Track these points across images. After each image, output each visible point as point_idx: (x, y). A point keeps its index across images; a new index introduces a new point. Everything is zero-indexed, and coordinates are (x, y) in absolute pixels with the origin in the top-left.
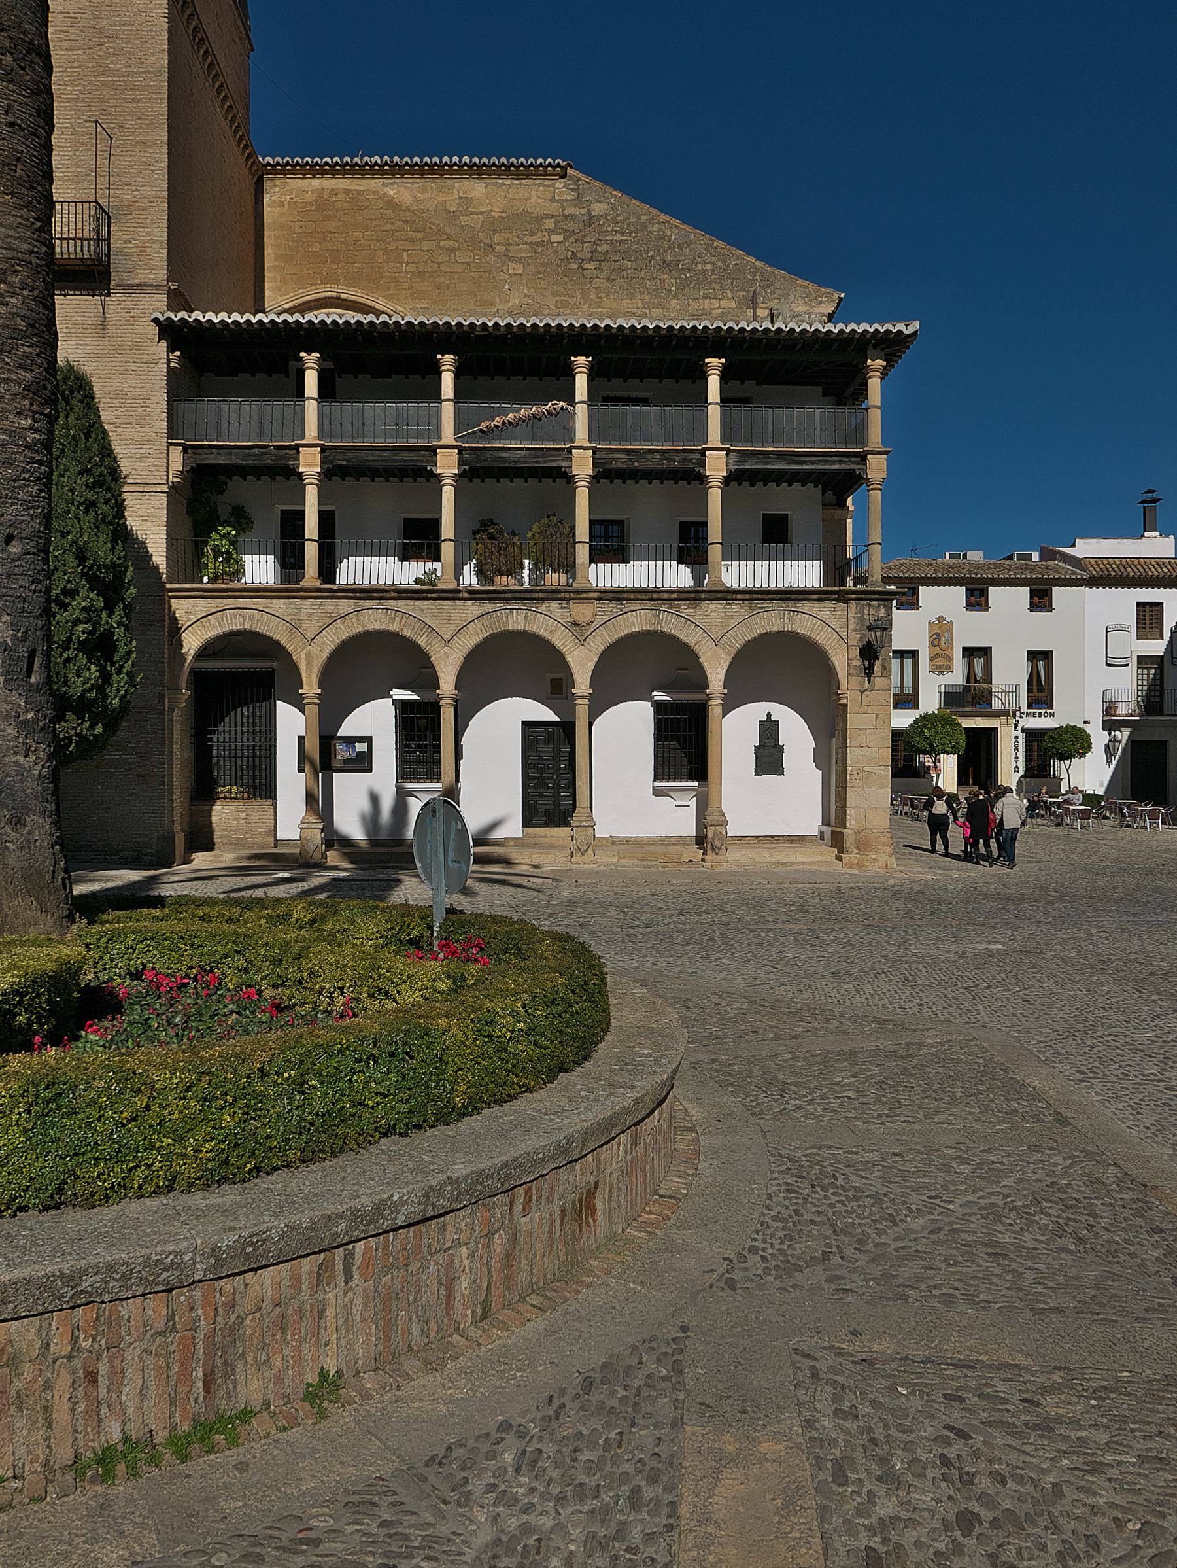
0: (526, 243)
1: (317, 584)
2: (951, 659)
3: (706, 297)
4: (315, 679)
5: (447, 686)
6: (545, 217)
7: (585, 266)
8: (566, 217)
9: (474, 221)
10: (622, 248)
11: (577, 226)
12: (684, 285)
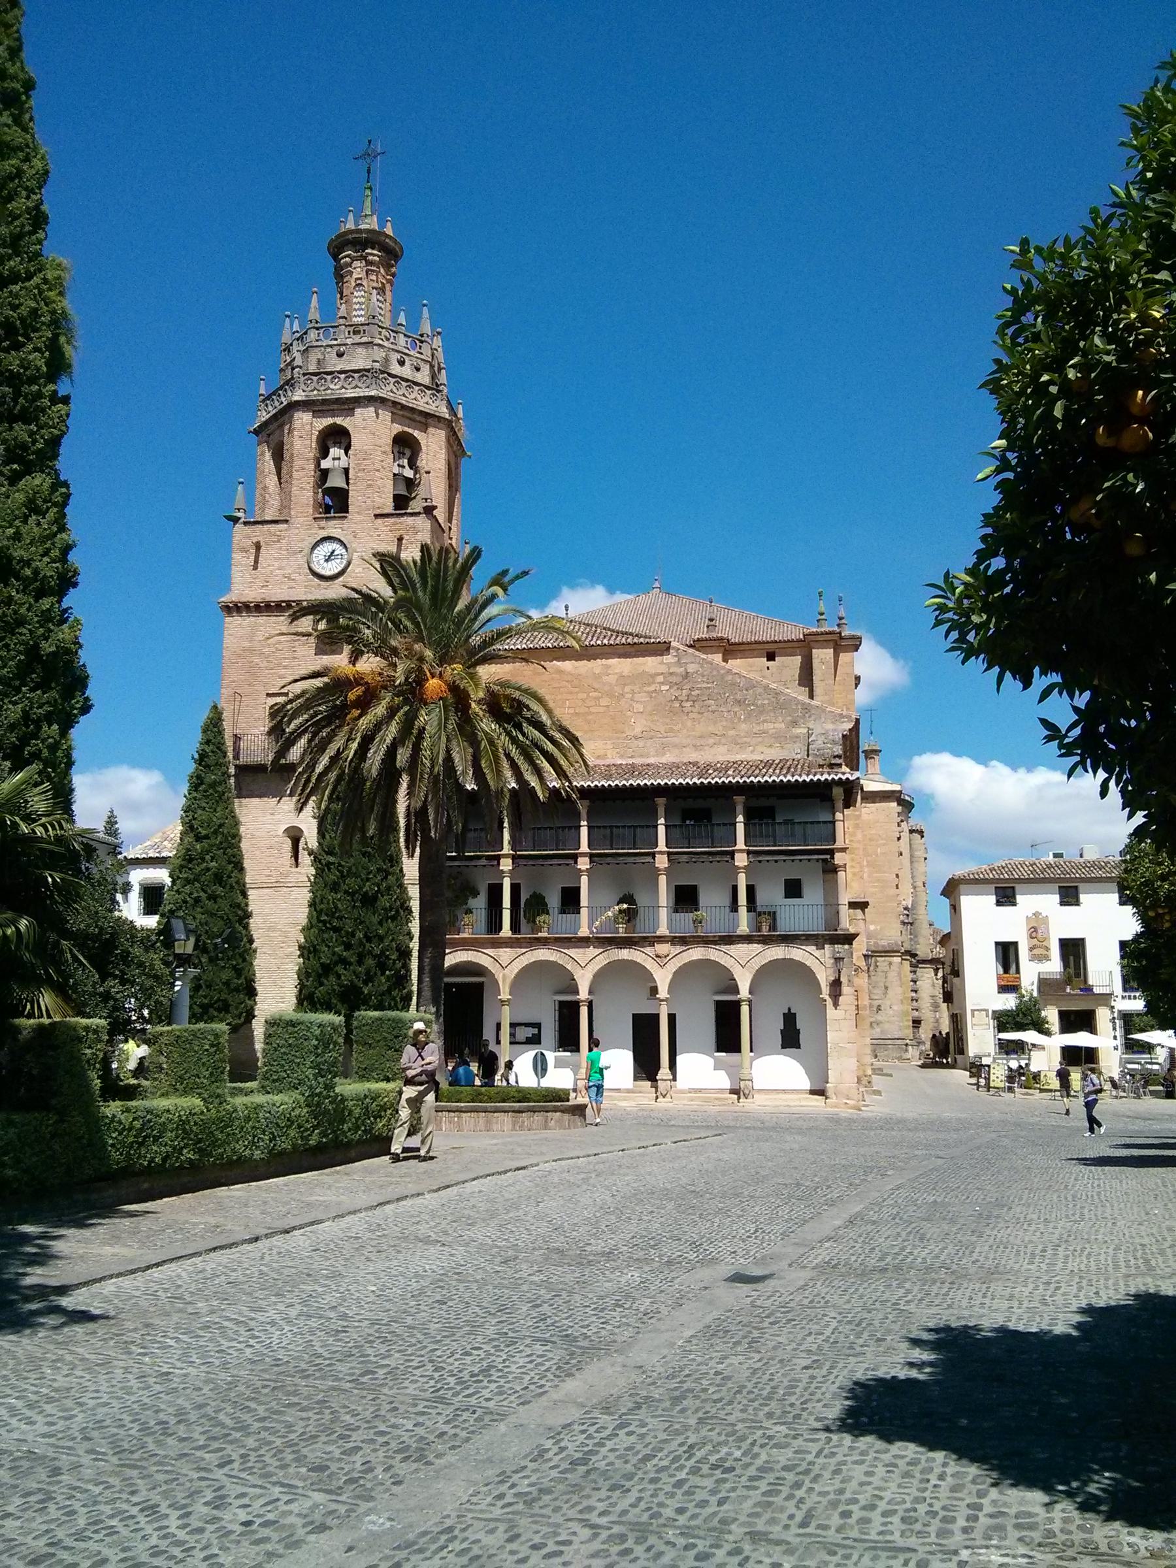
2: (1047, 949)
3: (765, 721)
4: (507, 990)
5: (583, 994)
6: (659, 674)
7: (684, 704)
8: (671, 674)
10: (708, 692)
11: (679, 679)
12: (749, 715)
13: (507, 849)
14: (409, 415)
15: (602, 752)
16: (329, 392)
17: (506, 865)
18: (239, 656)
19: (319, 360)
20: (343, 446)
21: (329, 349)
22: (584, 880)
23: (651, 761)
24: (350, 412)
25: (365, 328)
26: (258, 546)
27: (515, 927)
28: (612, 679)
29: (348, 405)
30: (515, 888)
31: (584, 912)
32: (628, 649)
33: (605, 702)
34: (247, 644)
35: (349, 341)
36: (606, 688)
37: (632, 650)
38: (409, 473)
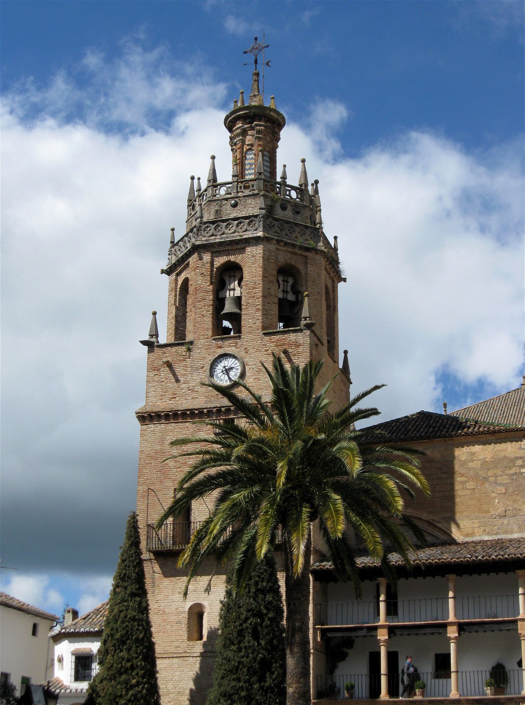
0: (506, 475)
1: (387, 698)
6: (517, 458)
9: (476, 464)
13: (382, 619)
14: (290, 250)
15: (470, 531)
16: (223, 236)
17: (382, 635)
18: (152, 458)
19: (217, 211)
20: (238, 277)
21: (224, 202)
22: (453, 646)
23: (516, 536)
24: (242, 250)
25: (252, 183)
26: (169, 365)
27: (393, 691)
28: (476, 464)
29: (240, 245)
30: (393, 658)
31: (453, 675)
32: (490, 437)
33: (471, 485)
34: (158, 448)
35: (240, 194)
36: (471, 473)
37: (493, 438)
38: (291, 297)
